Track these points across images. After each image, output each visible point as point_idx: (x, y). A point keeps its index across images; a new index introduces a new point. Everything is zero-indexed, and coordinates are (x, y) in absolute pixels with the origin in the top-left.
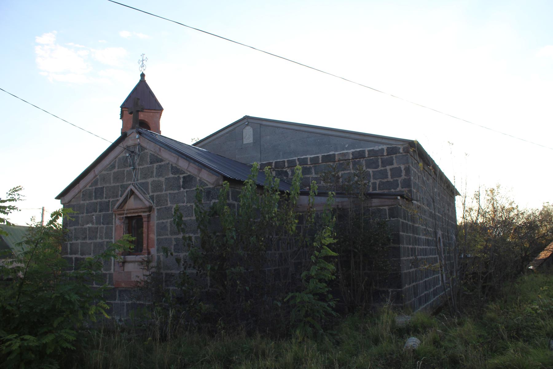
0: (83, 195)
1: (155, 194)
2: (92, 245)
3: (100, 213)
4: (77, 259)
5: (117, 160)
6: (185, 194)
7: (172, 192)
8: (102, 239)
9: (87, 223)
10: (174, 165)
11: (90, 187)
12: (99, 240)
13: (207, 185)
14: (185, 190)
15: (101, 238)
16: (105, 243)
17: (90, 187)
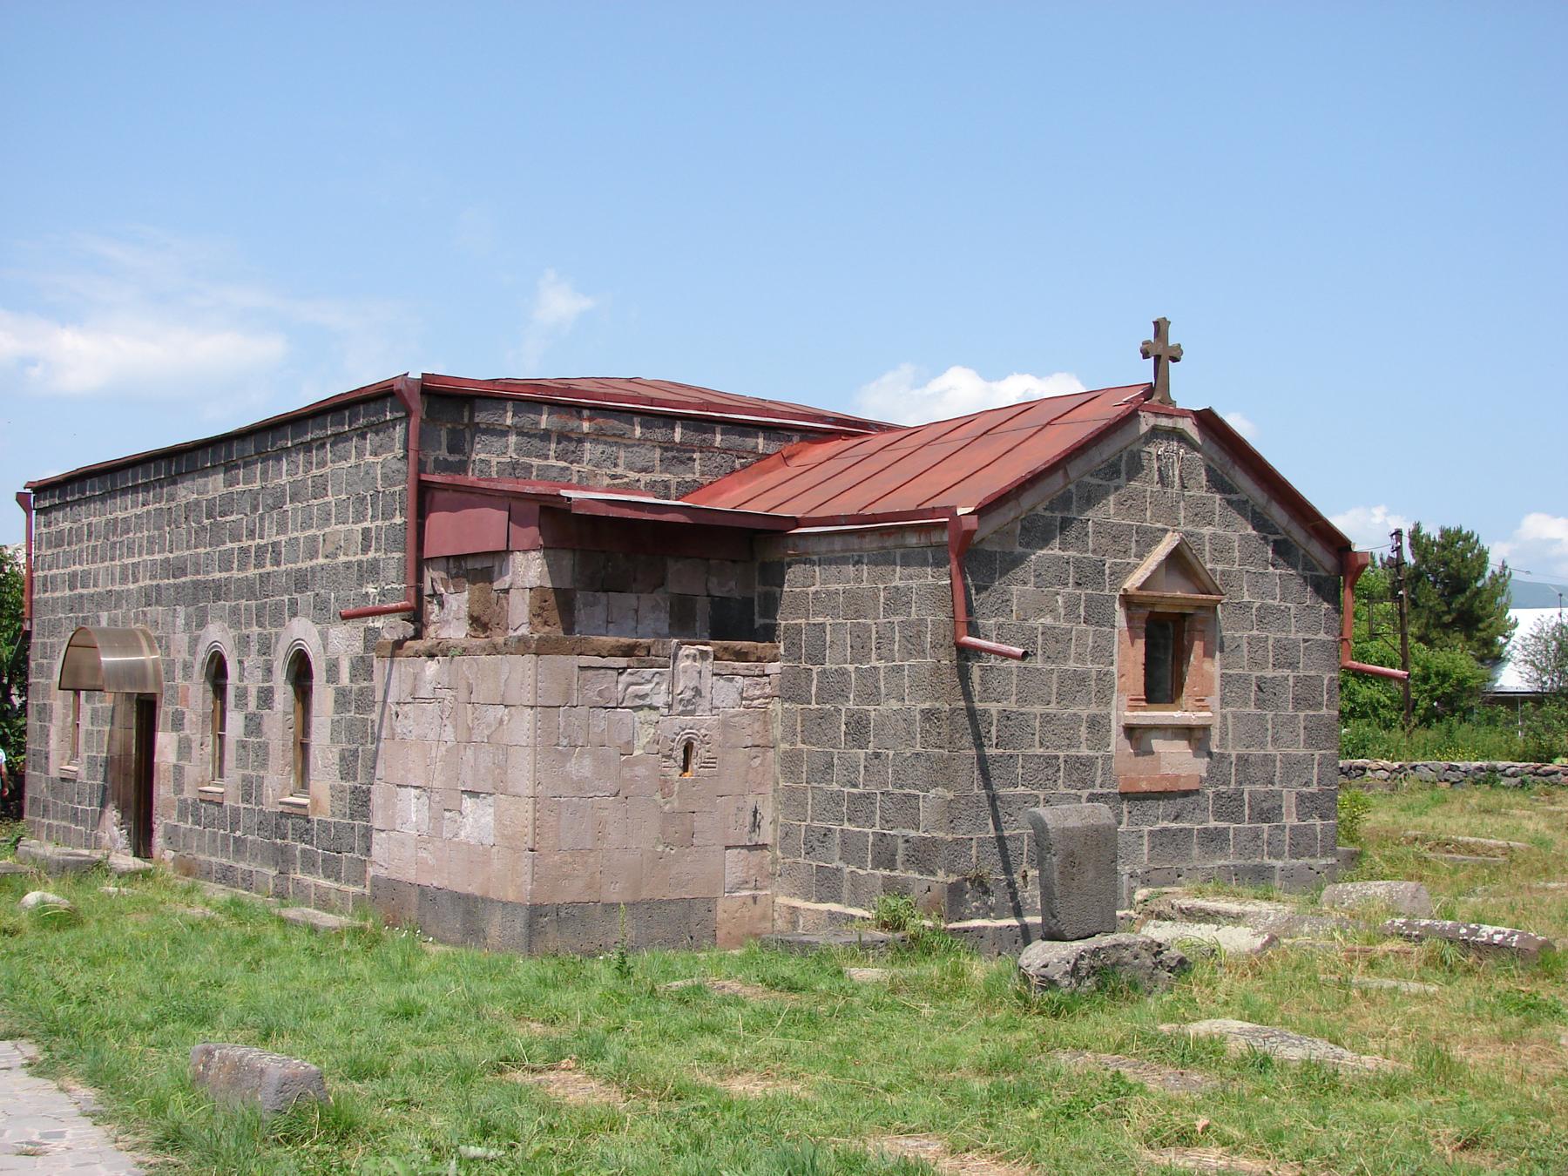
0: (1023, 528)
1: (1219, 567)
2: (1055, 676)
3: (1078, 592)
4: (1006, 716)
5: (1124, 458)
6: (1278, 581)
7: (1252, 569)
8: (1084, 662)
9: (1040, 612)
10: (1258, 510)
11: (1045, 509)
12: (1071, 665)
13: (1317, 570)
14: (1278, 571)
15: (1080, 658)
16: (1094, 674)
17: (1045, 509)
